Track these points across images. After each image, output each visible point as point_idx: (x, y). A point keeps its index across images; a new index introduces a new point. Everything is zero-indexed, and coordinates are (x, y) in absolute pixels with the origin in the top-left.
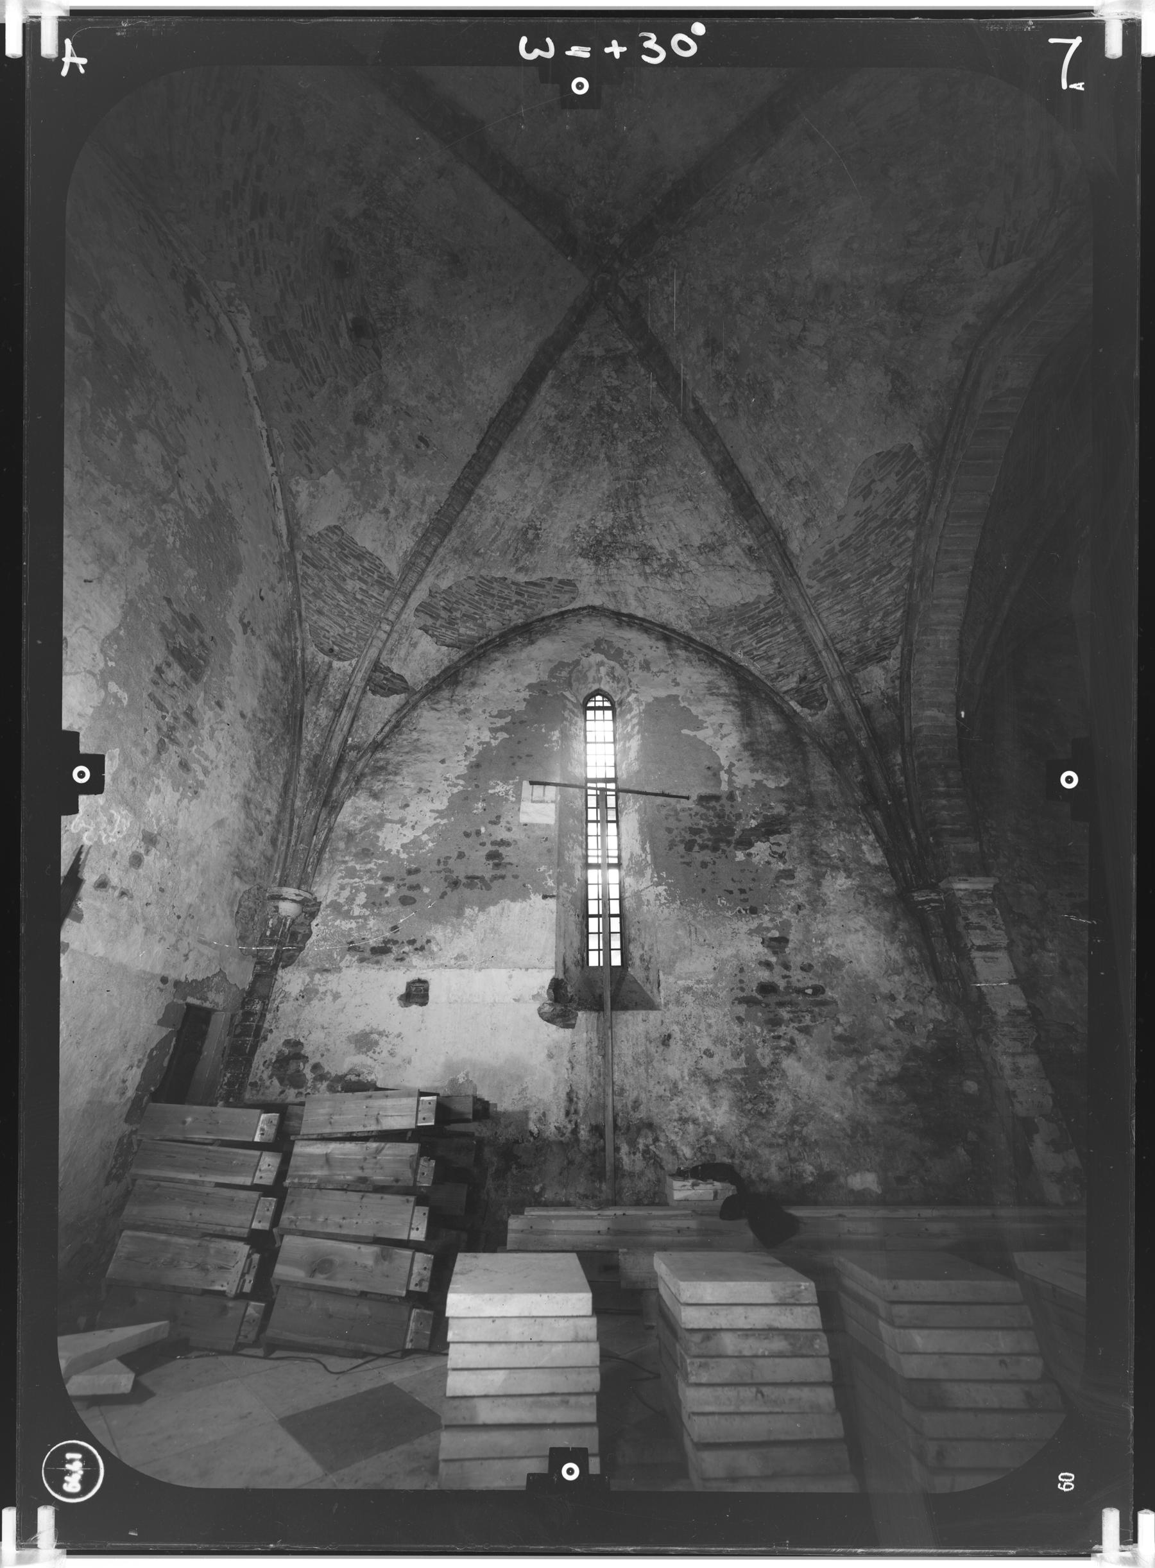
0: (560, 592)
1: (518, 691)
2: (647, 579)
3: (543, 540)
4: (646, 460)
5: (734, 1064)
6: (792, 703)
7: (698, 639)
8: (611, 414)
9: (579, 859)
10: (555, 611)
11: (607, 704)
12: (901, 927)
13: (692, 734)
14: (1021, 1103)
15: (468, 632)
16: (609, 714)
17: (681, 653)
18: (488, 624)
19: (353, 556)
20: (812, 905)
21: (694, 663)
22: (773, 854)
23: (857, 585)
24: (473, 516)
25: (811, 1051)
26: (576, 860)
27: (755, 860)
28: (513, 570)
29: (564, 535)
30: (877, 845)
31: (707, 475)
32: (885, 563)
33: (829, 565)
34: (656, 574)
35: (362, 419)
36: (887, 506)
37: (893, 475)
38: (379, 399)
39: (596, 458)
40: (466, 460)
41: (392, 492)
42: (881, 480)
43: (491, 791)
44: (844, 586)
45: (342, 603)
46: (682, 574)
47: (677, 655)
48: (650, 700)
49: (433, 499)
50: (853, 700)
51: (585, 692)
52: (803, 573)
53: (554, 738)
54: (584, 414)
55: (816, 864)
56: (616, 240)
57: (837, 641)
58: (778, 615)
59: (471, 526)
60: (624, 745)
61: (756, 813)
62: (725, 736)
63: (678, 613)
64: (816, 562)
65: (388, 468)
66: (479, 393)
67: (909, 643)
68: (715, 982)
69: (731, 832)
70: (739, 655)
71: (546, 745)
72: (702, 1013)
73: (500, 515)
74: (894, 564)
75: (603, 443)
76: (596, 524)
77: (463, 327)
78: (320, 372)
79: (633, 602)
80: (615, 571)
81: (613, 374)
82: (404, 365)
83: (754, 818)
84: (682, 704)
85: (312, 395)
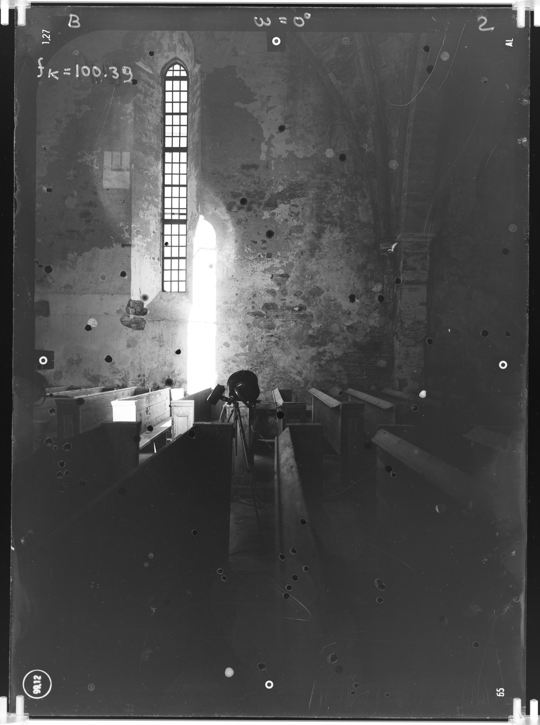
5: (241, 350)
6: (331, 75)
9: (155, 216)
11: (184, 74)
12: (368, 267)
13: (243, 106)
14: (402, 372)
16: (184, 84)
20: (311, 251)
22: (291, 213)
25: (290, 343)
26: (151, 217)
27: (277, 218)
30: (370, 206)
43: (80, 161)
51: (162, 62)
53: (129, 111)
55: (321, 222)
60: (192, 116)
61: (284, 180)
68: (236, 303)
69: (261, 195)
71: (122, 118)
72: (225, 322)
83: (281, 184)
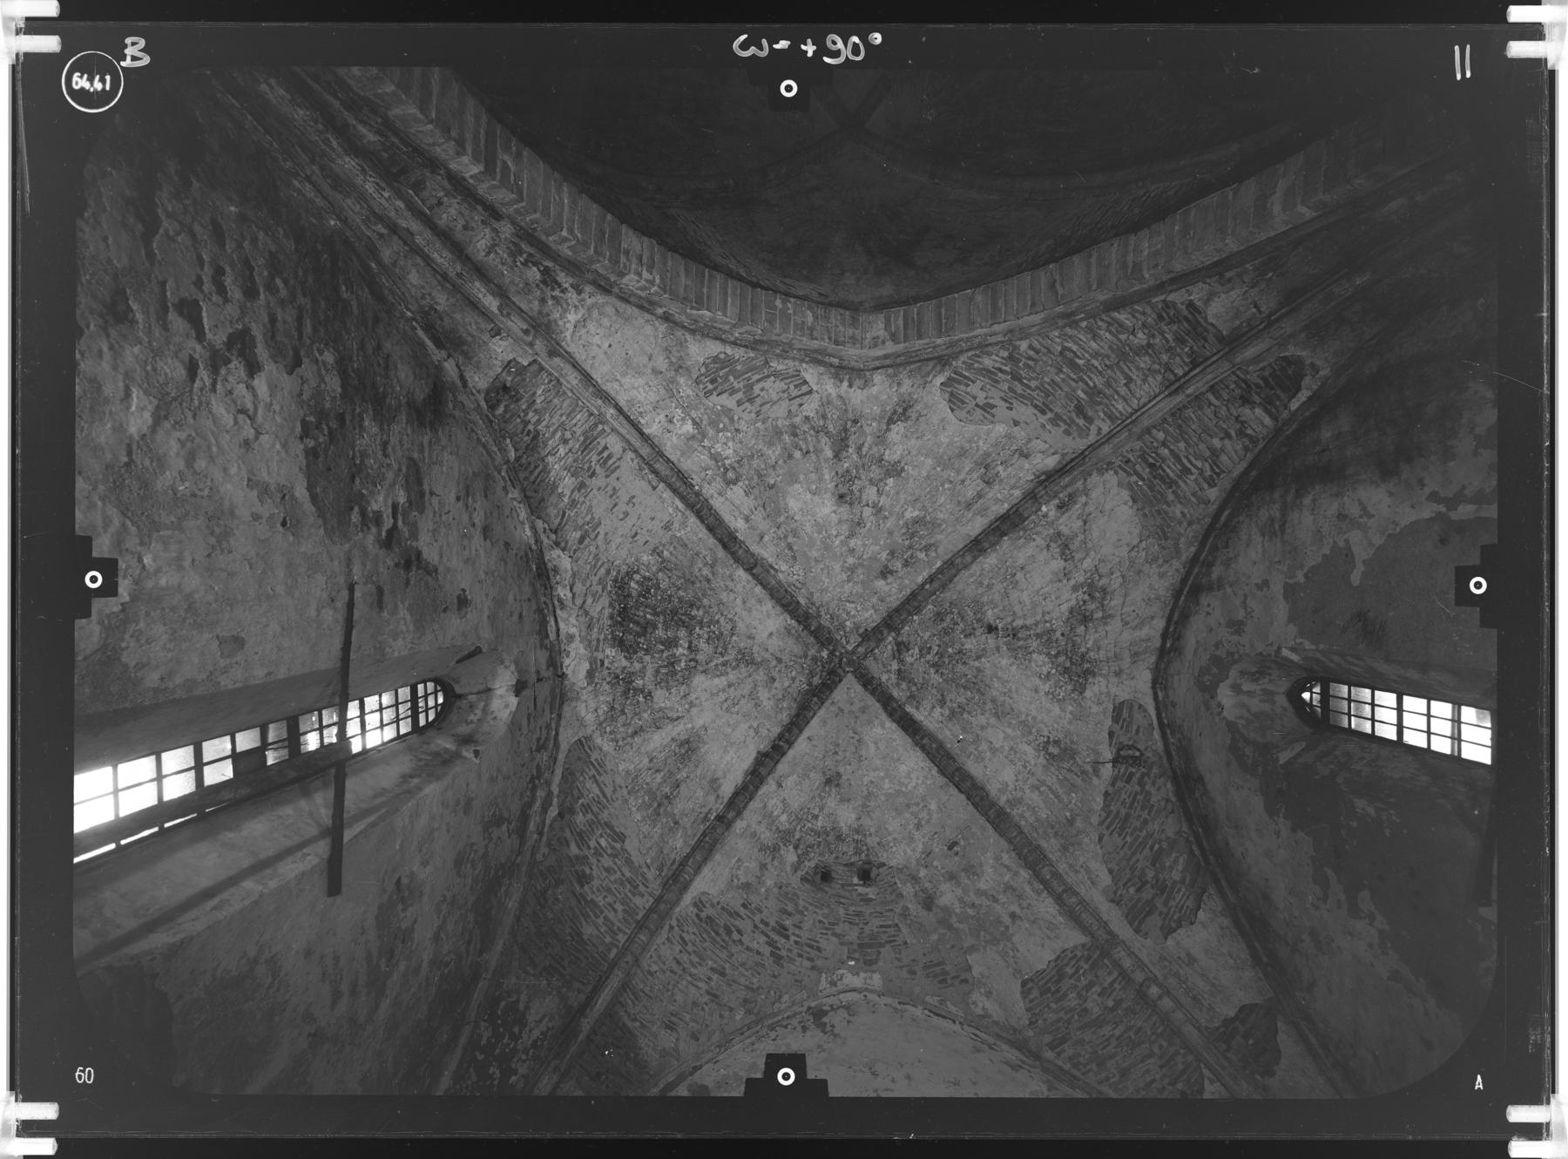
0: (1130, 723)
1: (1278, 833)
2: (1110, 616)
3: (1061, 736)
4: (979, 621)
6: (1294, 405)
7: (1193, 549)
8: (941, 655)
10: (1157, 734)
13: (1359, 569)
15: (1180, 868)
17: (1217, 571)
18: (1170, 833)
19: (1059, 981)
21: (1231, 555)
23: (1091, 379)
24: (1027, 814)
28: (1096, 781)
29: (1056, 710)
31: (990, 561)
32: (1059, 359)
33: (1070, 418)
34: (1103, 606)
35: (928, 902)
36: (997, 382)
37: (969, 389)
38: (915, 879)
39: (978, 670)
40: (971, 808)
41: (996, 900)
42: (975, 398)
44: (1093, 392)
45: (1117, 1032)
46: (1101, 577)
47: (1220, 578)
48: (1292, 629)
49: (1005, 856)
50: (1270, 324)
52: (1081, 444)
53: (1371, 811)
54: (941, 680)
56: (825, 654)
57: (1172, 377)
58: (1143, 457)
59: (1037, 820)
62: (1364, 509)
63: (1156, 577)
64: (1067, 433)
65: (971, 894)
66: (918, 779)
67: (1160, 287)
70: (1213, 494)
73: (1029, 782)
74: (1059, 348)
75: (964, 663)
76: (1045, 672)
77: (872, 782)
78: (889, 926)
79: (1145, 632)
80: (1101, 652)
81: (910, 652)
82: (892, 844)
84: (1301, 578)
85: (906, 943)
